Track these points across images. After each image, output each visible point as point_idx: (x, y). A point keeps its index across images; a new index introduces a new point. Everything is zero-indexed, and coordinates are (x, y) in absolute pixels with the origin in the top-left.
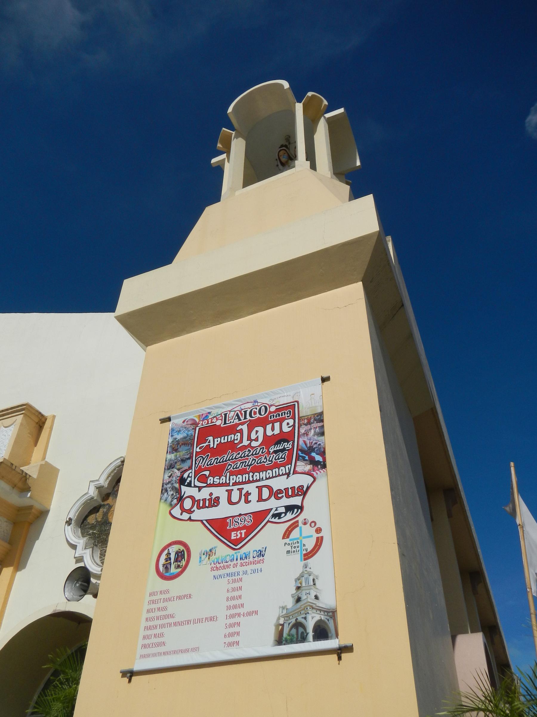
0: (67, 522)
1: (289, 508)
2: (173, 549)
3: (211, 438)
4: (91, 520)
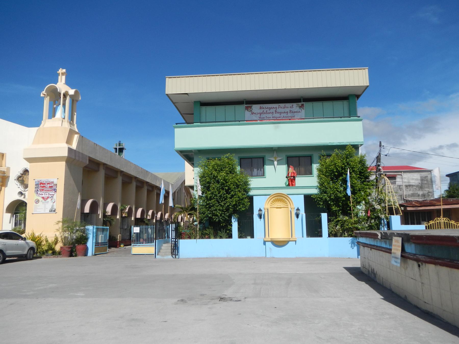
1: (52, 197)
2: (37, 200)
3: (41, 185)
4: (20, 179)
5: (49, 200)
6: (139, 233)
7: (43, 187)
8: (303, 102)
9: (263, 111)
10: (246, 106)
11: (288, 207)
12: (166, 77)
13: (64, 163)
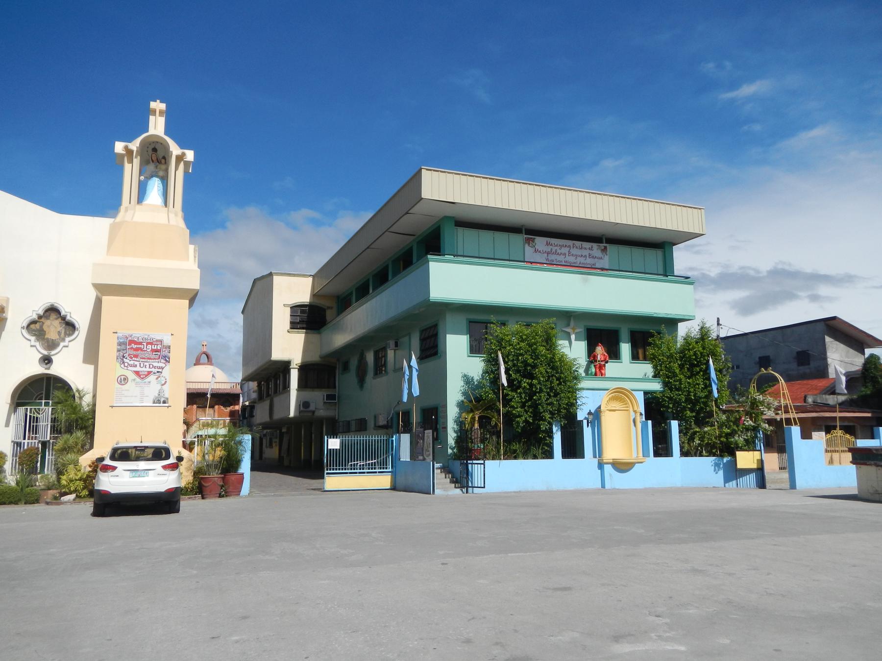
0: (22, 328)
1: (158, 372)
2: (122, 377)
3: (133, 344)
4: (32, 326)
5: (152, 378)
6: (339, 450)
7: (137, 349)
8: (606, 243)
9: (552, 249)
10: (525, 238)
11: (627, 410)
12: (422, 167)
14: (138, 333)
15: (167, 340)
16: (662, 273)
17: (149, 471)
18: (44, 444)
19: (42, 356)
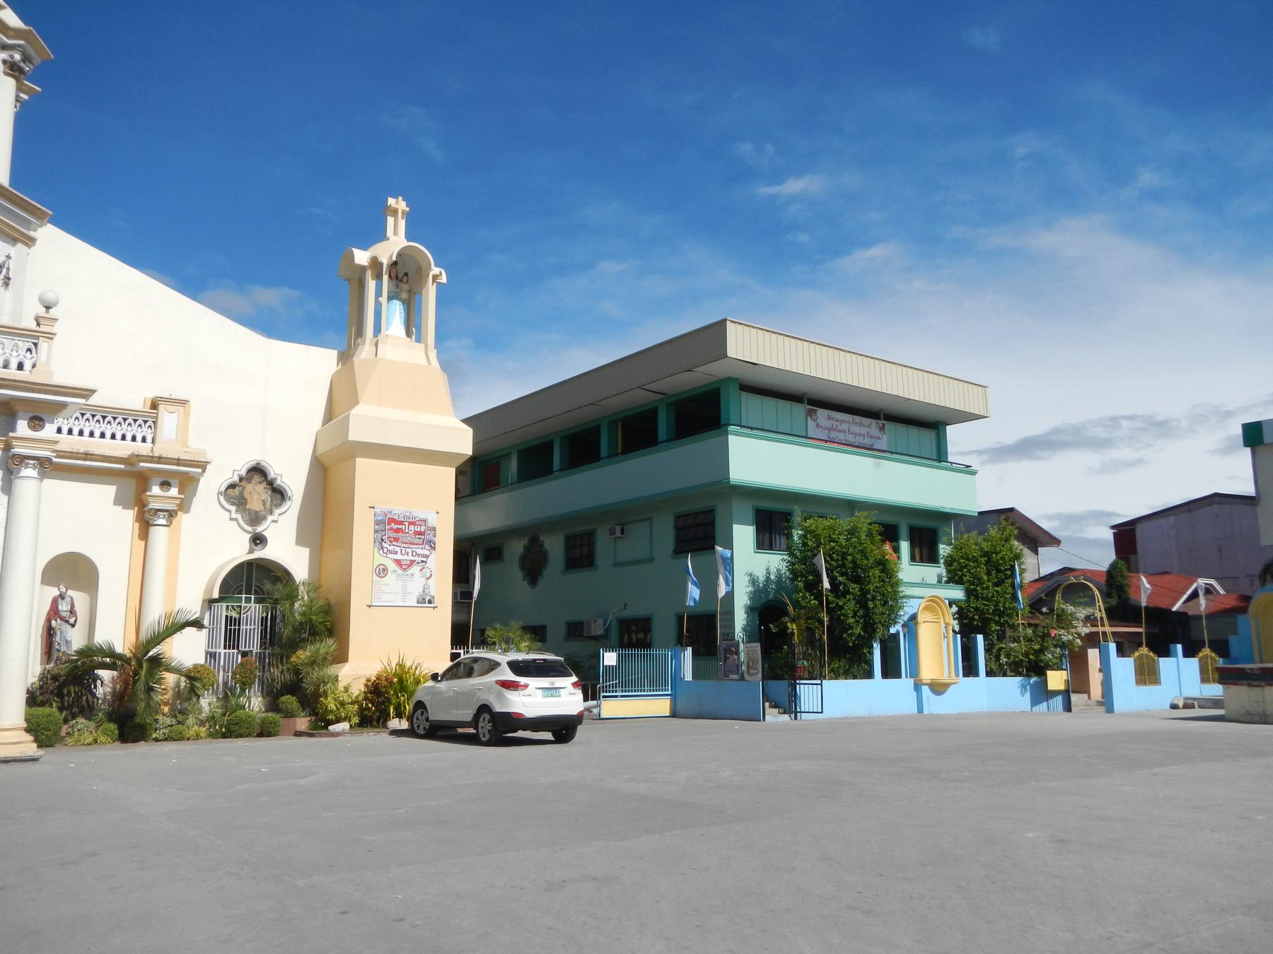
0: (219, 493)
1: (422, 561)
2: (381, 567)
3: (393, 524)
4: (230, 491)
5: (415, 569)
6: (616, 666)
7: (398, 531)
8: (885, 420)
13: (451, 472)
14: (399, 509)
15: (432, 520)
16: (935, 458)
17: (561, 690)
18: (244, 654)
19: (250, 535)
